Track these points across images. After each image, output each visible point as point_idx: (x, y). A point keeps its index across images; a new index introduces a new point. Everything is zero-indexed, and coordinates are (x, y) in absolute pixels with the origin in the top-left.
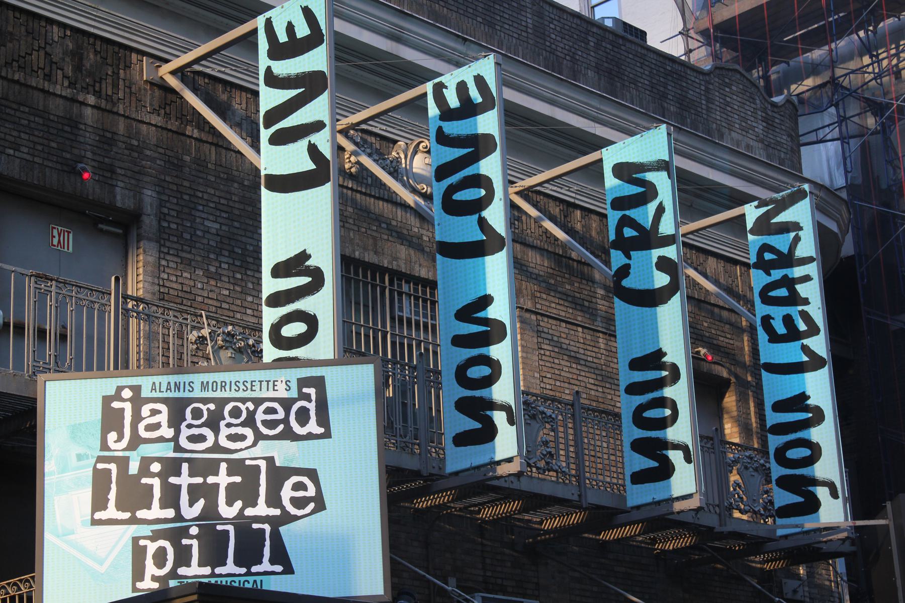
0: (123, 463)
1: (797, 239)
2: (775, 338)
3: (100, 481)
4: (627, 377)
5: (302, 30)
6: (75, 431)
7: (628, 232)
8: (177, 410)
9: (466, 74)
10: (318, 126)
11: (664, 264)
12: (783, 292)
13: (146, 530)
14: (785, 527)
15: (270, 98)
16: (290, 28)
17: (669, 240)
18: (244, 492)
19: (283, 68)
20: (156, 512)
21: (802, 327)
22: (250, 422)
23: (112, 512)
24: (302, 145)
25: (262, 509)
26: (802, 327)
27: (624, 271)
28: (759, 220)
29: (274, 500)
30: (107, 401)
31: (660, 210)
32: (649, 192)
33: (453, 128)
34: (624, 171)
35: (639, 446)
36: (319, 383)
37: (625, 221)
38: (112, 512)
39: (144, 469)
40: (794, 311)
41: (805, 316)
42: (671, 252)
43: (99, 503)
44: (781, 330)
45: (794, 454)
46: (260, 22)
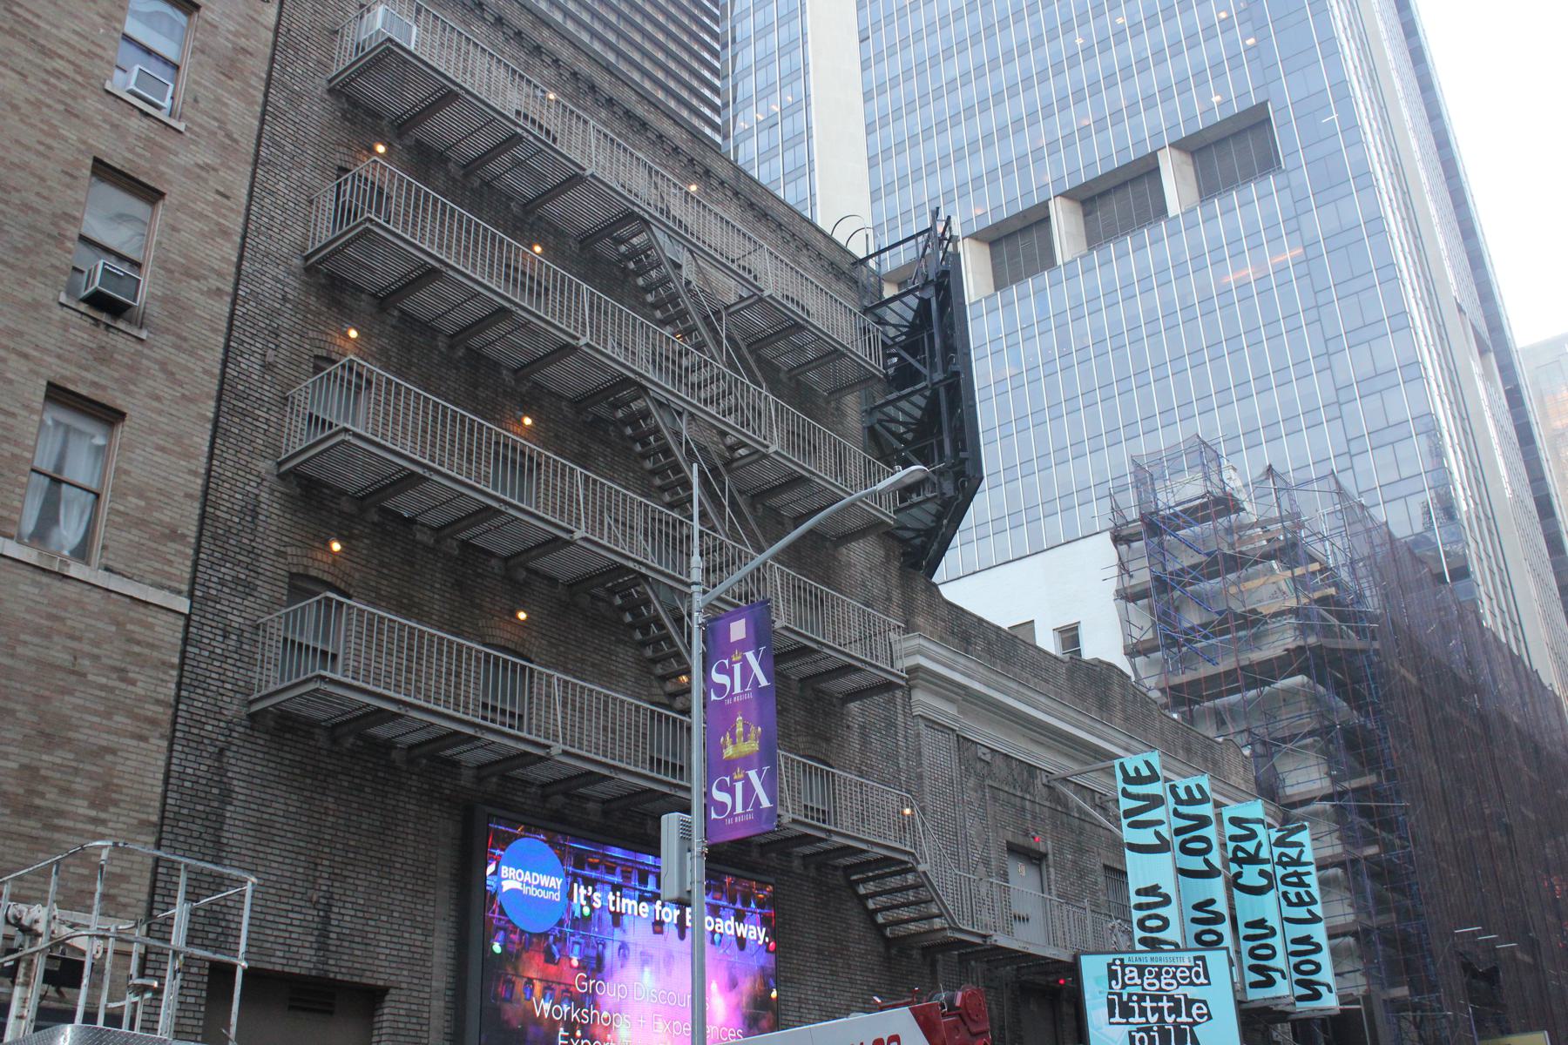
0: (1120, 995)
1: (1301, 852)
2: (1290, 904)
3: (1111, 1004)
4: (1135, 900)
5: (1145, 772)
6: (1097, 980)
7: (1240, 854)
8: (1141, 969)
9: (1192, 782)
10: (1161, 822)
11: (1262, 873)
12: (1294, 880)
13: (1134, 1028)
14: (1301, 1006)
15: (1126, 804)
16: (1137, 770)
17: (1266, 861)
18: (1176, 1010)
19: (1132, 789)
20: (1137, 1019)
21: (1307, 899)
22: (1174, 977)
23: (1117, 1019)
24: (1151, 830)
25: (1184, 1019)
26: (1307, 899)
27: (1239, 875)
28: (1278, 839)
29: (1189, 1015)
30: (1109, 965)
31: (1259, 845)
32: (1253, 835)
33: (1183, 809)
34: (1236, 821)
35: (1252, 968)
36: (1203, 959)
37: (1237, 849)
38: (1117, 1019)
39: (1129, 999)
40: (1302, 890)
41: (1308, 893)
42: (1268, 868)
43: (1111, 1015)
44: (1294, 900)
45: (1304, 967)
46: (1117, 763)
